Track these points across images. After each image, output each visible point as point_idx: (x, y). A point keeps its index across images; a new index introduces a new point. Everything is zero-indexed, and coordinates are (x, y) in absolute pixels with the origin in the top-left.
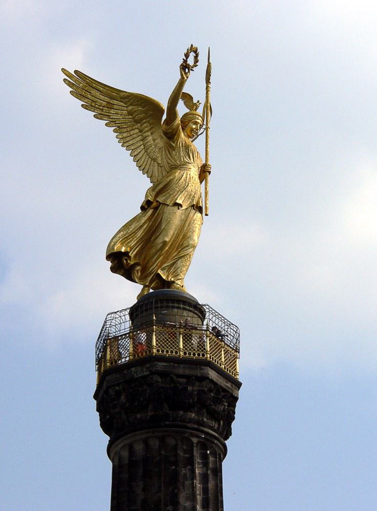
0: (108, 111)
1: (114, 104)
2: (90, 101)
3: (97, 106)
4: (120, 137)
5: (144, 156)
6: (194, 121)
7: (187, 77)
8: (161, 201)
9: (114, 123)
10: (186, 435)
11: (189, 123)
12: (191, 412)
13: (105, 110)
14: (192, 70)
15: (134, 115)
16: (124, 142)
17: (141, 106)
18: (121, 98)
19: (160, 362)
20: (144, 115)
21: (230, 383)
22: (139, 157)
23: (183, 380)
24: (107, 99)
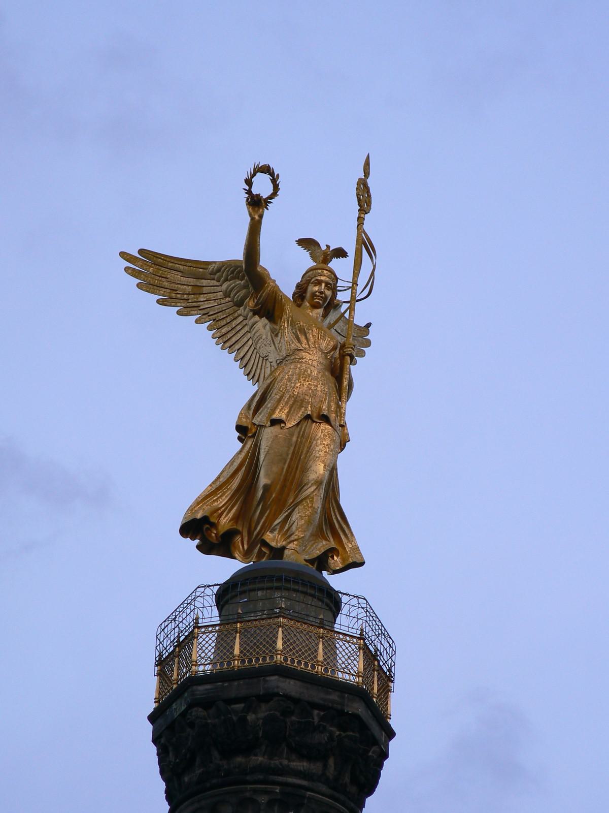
0: (195, 300)
1: (203, 286)
2: (168, 291)
3: (179, 296)
4: (219, 335)
5: (254, 356)
6: (313, 280)
7: (261, 216)
8: (257, 423)
9: (207, 315)
10: (248, 794)
11: (308, 285)
12: (256, 755)
13: (192, 299)
14: (271, 203)
15: (232, 296)
16: (226, 340)
17: (238, 278)
18: (211, 274)
19: (200, 684)
20: (244, 291)
21: (338, 693)
22: (247, 358)
23: (239, 706)
24: (192, 281)
